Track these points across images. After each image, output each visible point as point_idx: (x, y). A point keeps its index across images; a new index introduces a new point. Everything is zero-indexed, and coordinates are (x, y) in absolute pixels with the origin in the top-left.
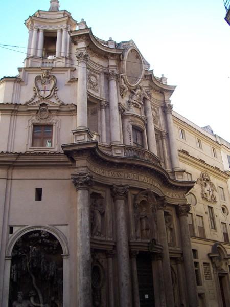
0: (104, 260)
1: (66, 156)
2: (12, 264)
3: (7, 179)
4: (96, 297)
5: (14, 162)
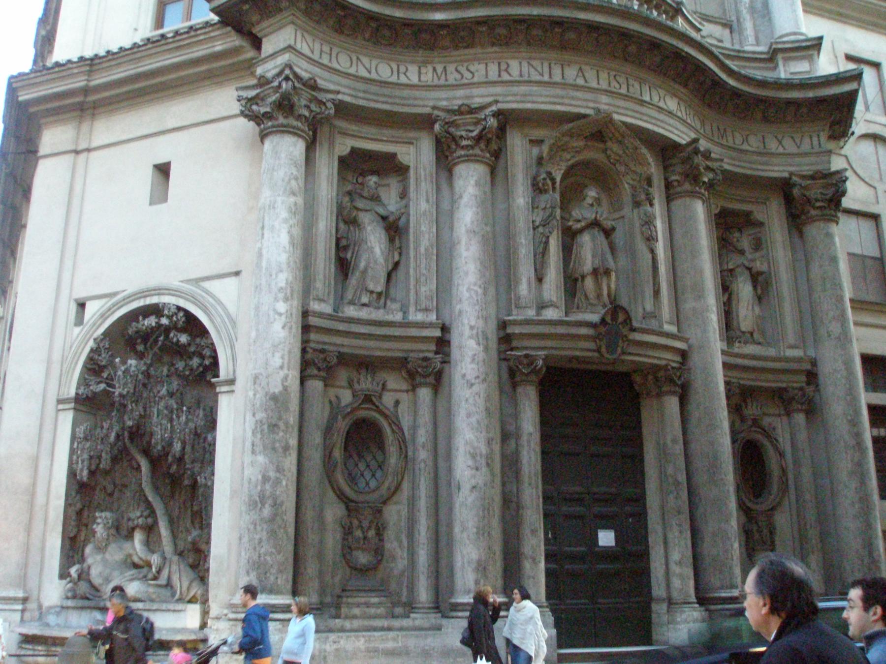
0: (404, 398)
1: (229, 29)
3: (77, 152)
4: (358, 533)
5: (86, 91)
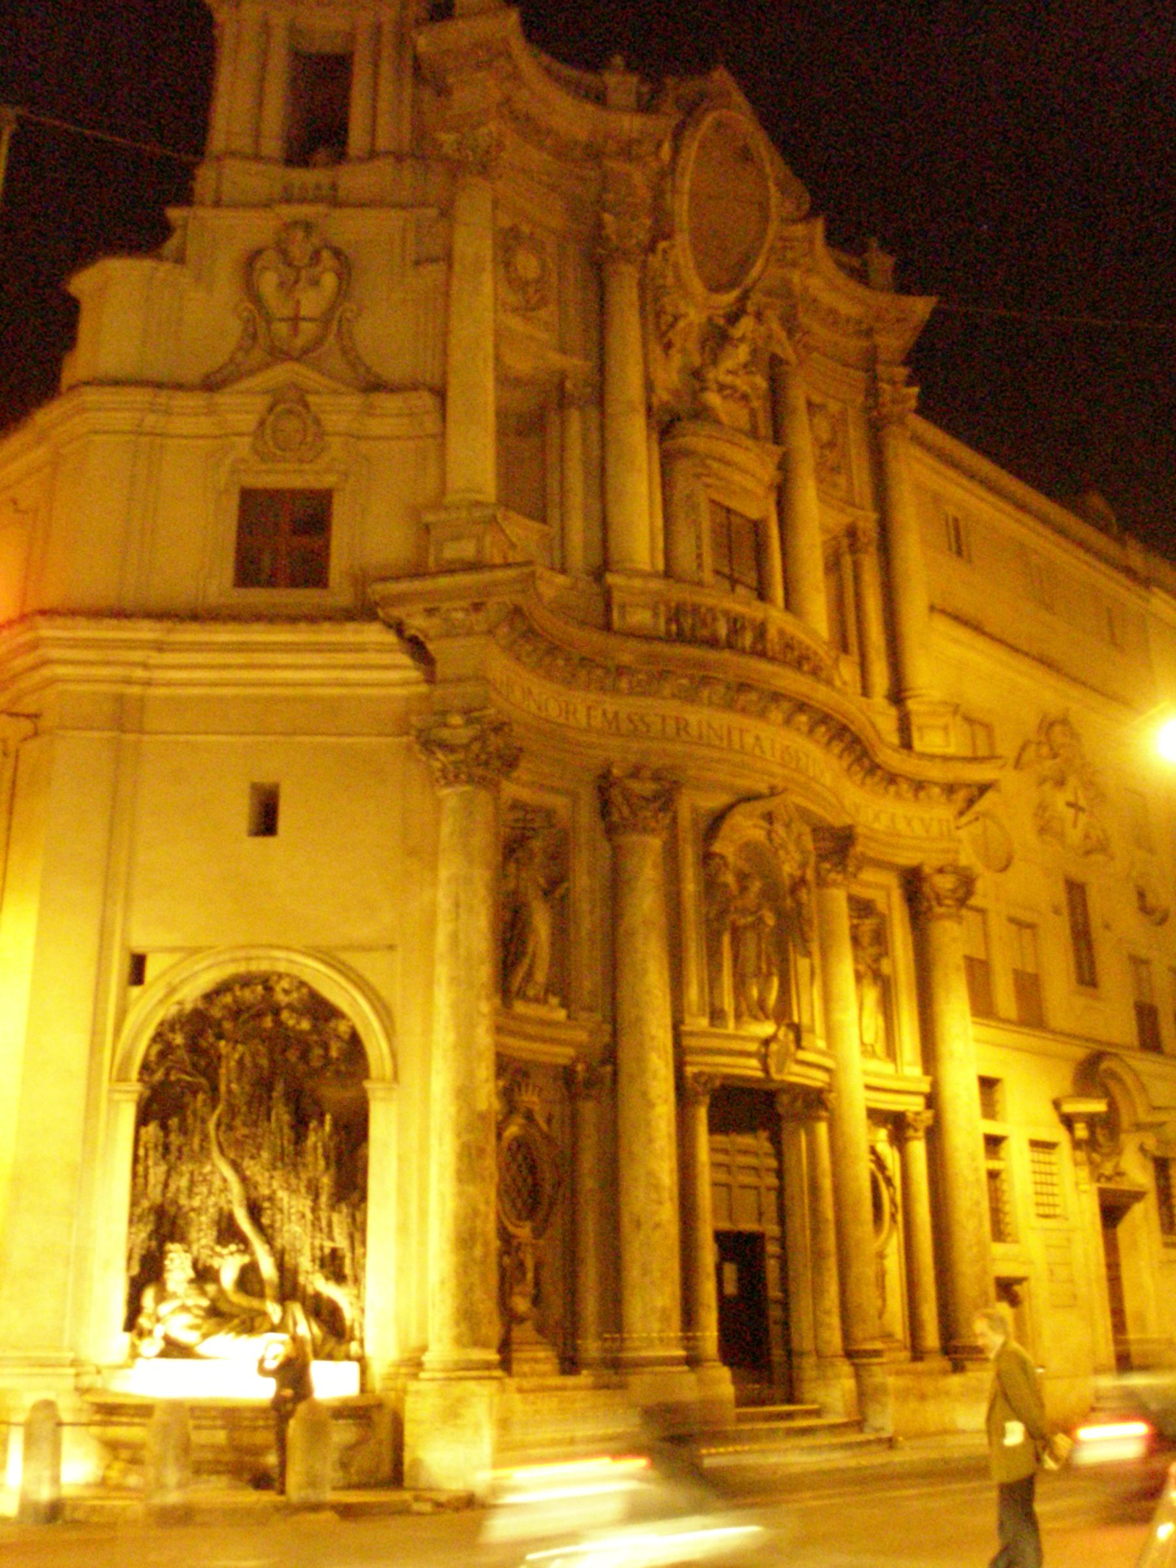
2: (142, 1120)
